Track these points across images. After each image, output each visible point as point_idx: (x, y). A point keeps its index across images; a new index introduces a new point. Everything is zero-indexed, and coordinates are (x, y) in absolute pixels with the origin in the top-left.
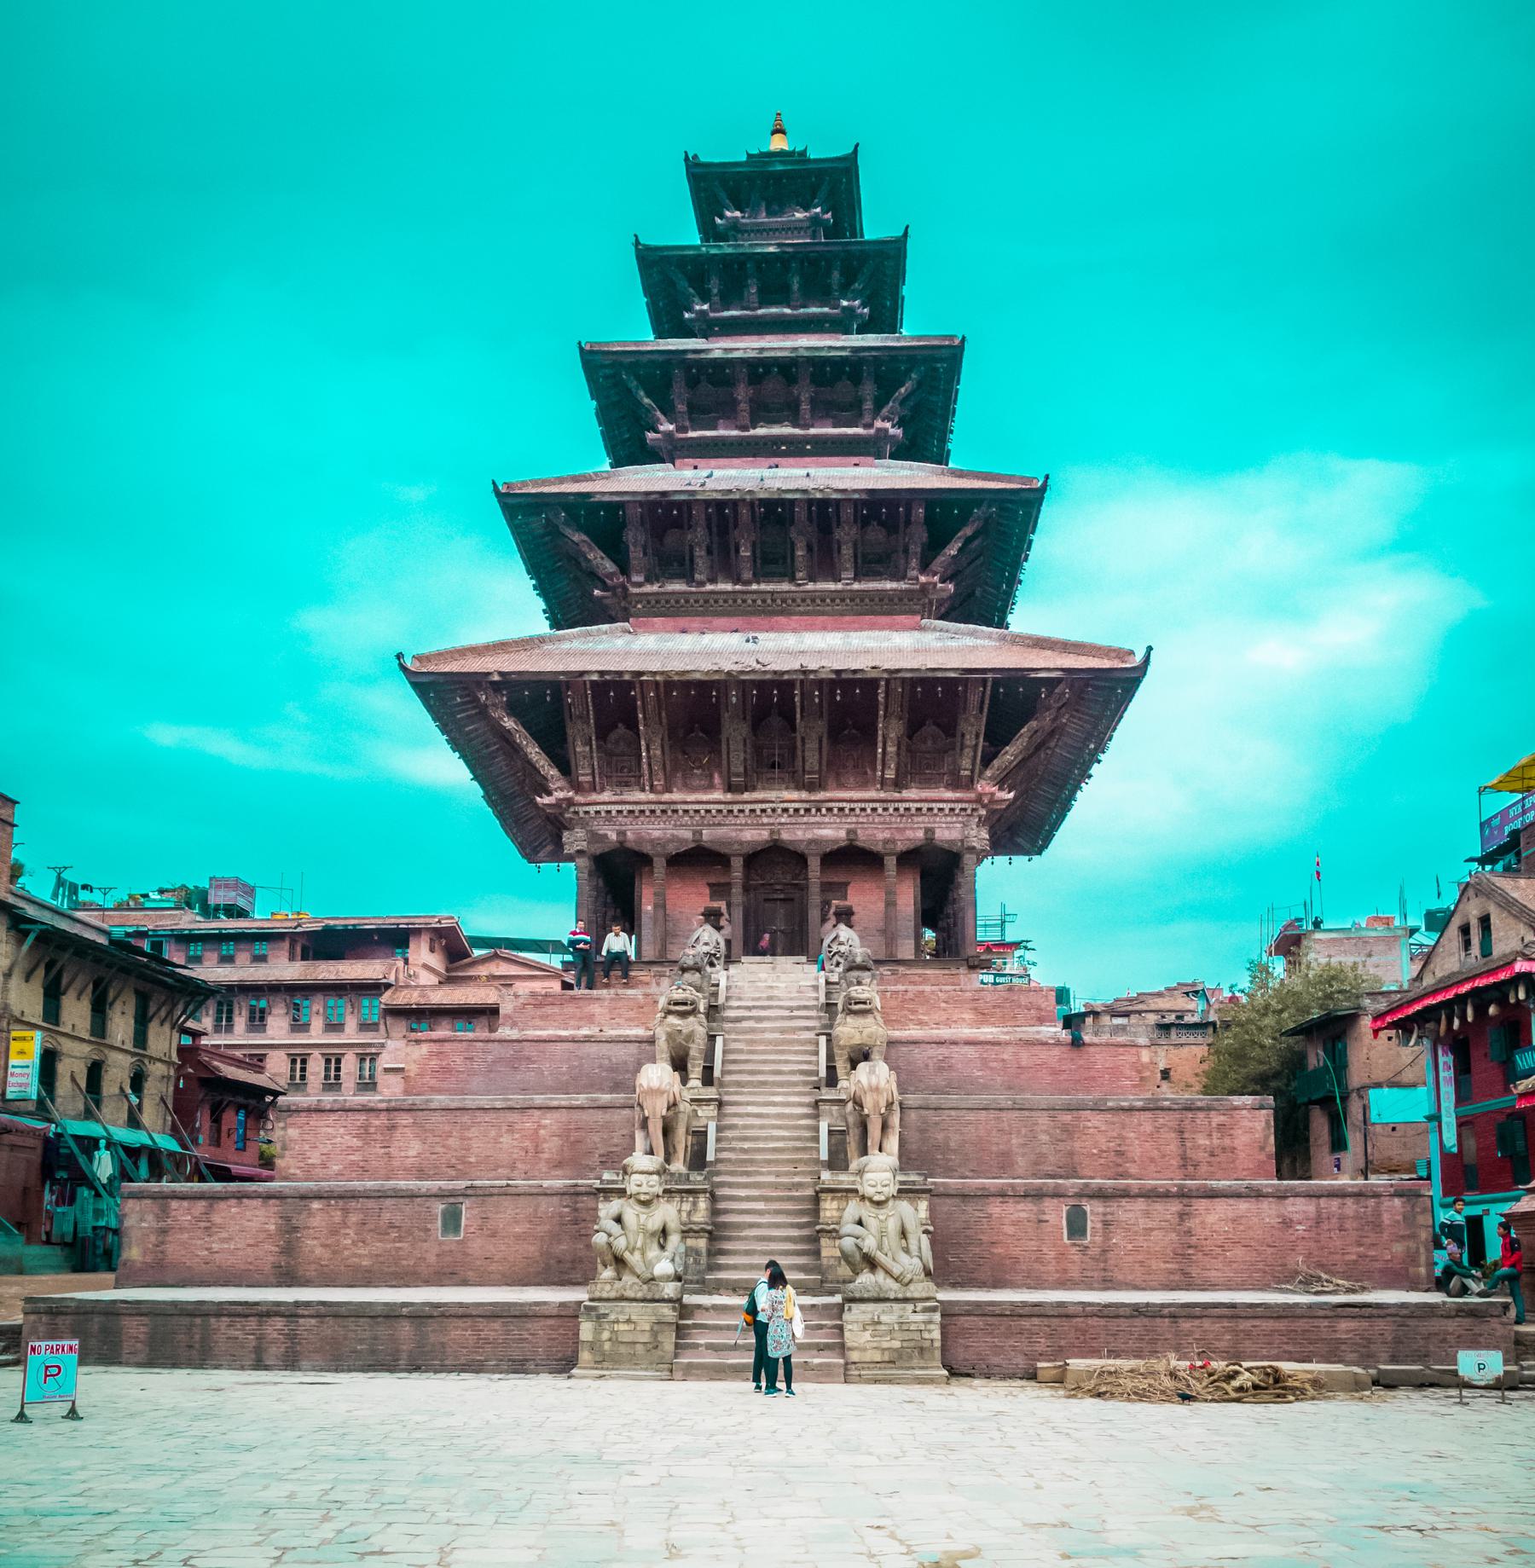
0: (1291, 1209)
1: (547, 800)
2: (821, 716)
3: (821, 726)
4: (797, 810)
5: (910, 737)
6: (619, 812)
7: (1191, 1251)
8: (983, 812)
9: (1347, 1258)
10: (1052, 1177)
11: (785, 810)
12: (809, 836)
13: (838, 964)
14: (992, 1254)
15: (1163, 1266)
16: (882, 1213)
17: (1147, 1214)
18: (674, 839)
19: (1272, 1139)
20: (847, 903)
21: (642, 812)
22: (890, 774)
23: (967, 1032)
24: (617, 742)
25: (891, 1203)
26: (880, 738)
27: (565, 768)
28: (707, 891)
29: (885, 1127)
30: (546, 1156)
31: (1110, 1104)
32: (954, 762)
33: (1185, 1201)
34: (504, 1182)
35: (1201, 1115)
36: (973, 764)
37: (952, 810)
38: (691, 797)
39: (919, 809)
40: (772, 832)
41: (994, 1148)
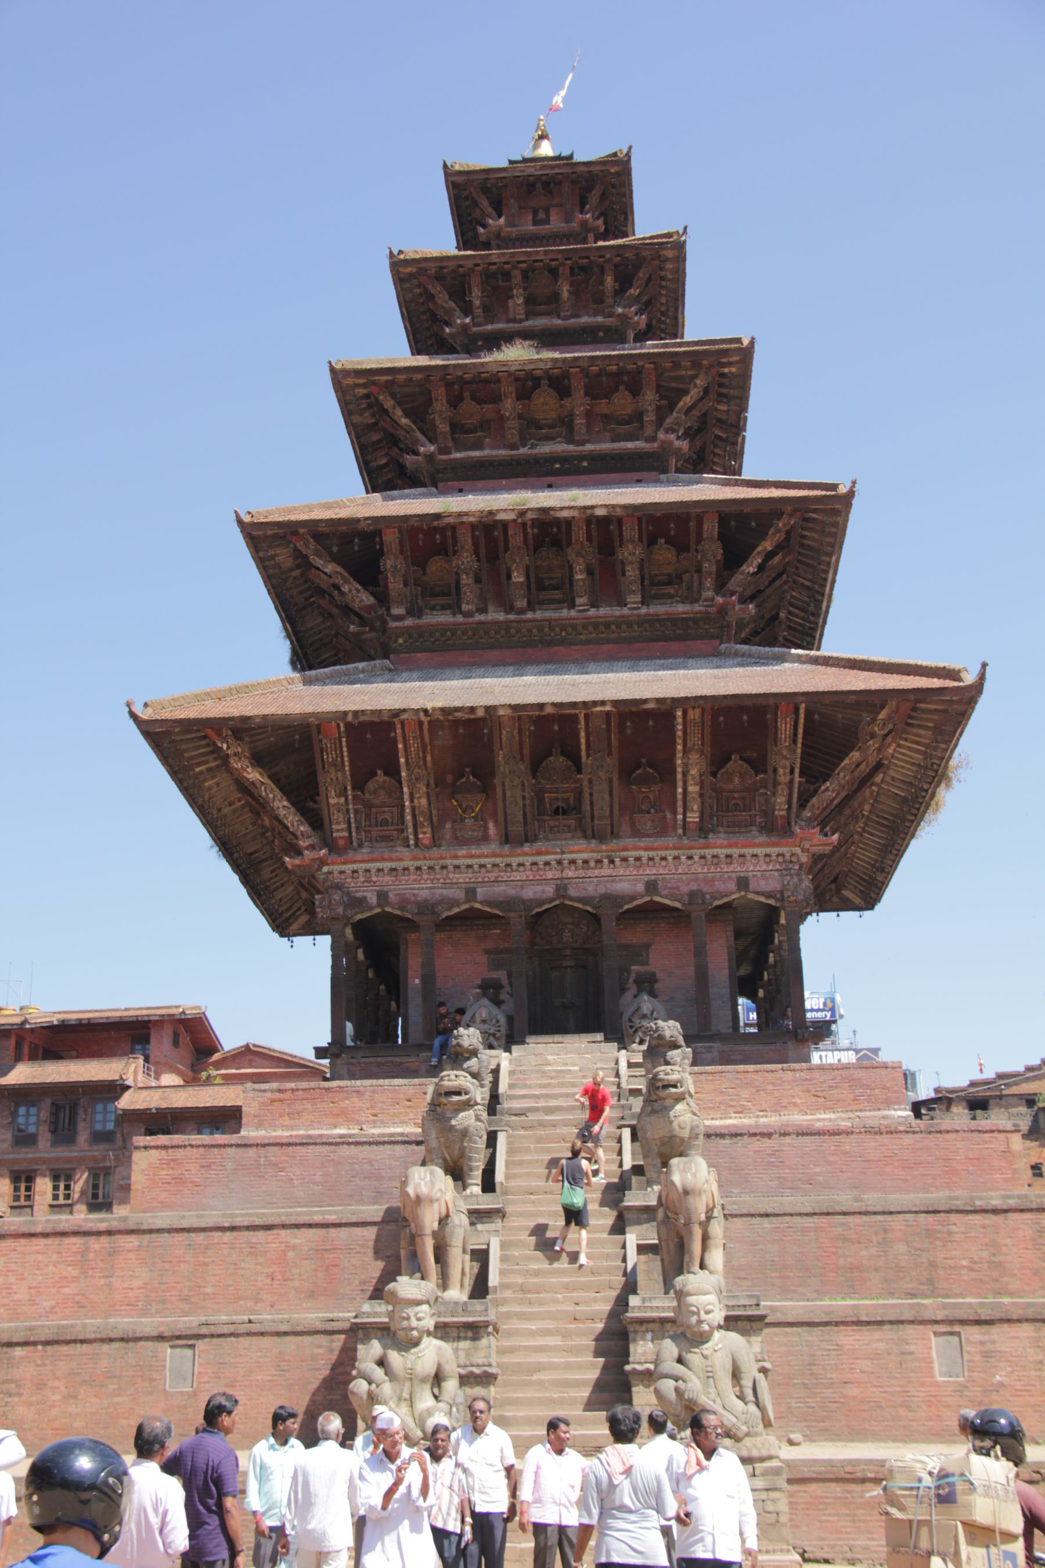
1: (297, 862)
2: (610, 753)
3: (611, 762)
4: (586, 862)
5: (714, 774)
6: (379, 870)
10: (913, 1296)
11: (573, 862)
12: (601, 890)
13: (641, 1042)
14: (845, 1397)
16: (707, 1348)
20: (649, 969)
21: (405, 869)
22: (693, 817)
23: (798, 1118)
25: (717, 1335)
26: (679, 777)
27: (316, 821)
28: (484, 959)
29: (705, 1238)
30: (296, 1284)
31: (978, 1203)
32: (767, 801)
34: (246, 1318)
37: (767, 855)
39: (729, 856)
40: (558, 888)
41: (841, 1262)
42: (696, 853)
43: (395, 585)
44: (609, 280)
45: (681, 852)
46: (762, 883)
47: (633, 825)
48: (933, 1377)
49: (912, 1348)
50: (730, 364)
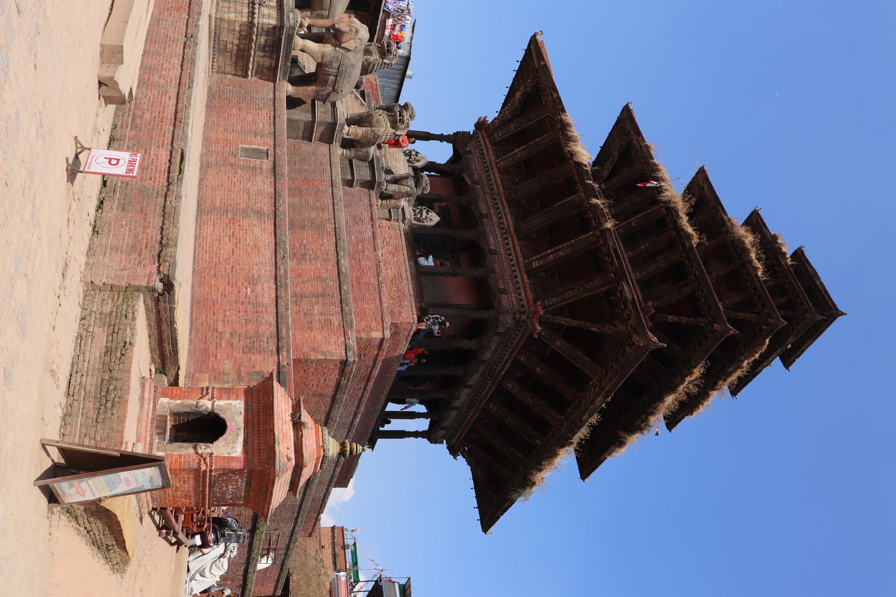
0: (265, 284)
4: (502, 223)
9: (220, 324)
11: (501, 218)
12: (488, 232)
15: (218, 198)
17: (260, 193)
19: (323, 357)
22: (535, 264)
31: (342, 253)
33: (272, 216)
35: (338, 309)
36: (554, 304)
37: (521, 300)
39: (517, 283)
41: (304, 187)
44: (783, 300)
46: (505, 301)
49: (259, 138)
50: (768, 325)
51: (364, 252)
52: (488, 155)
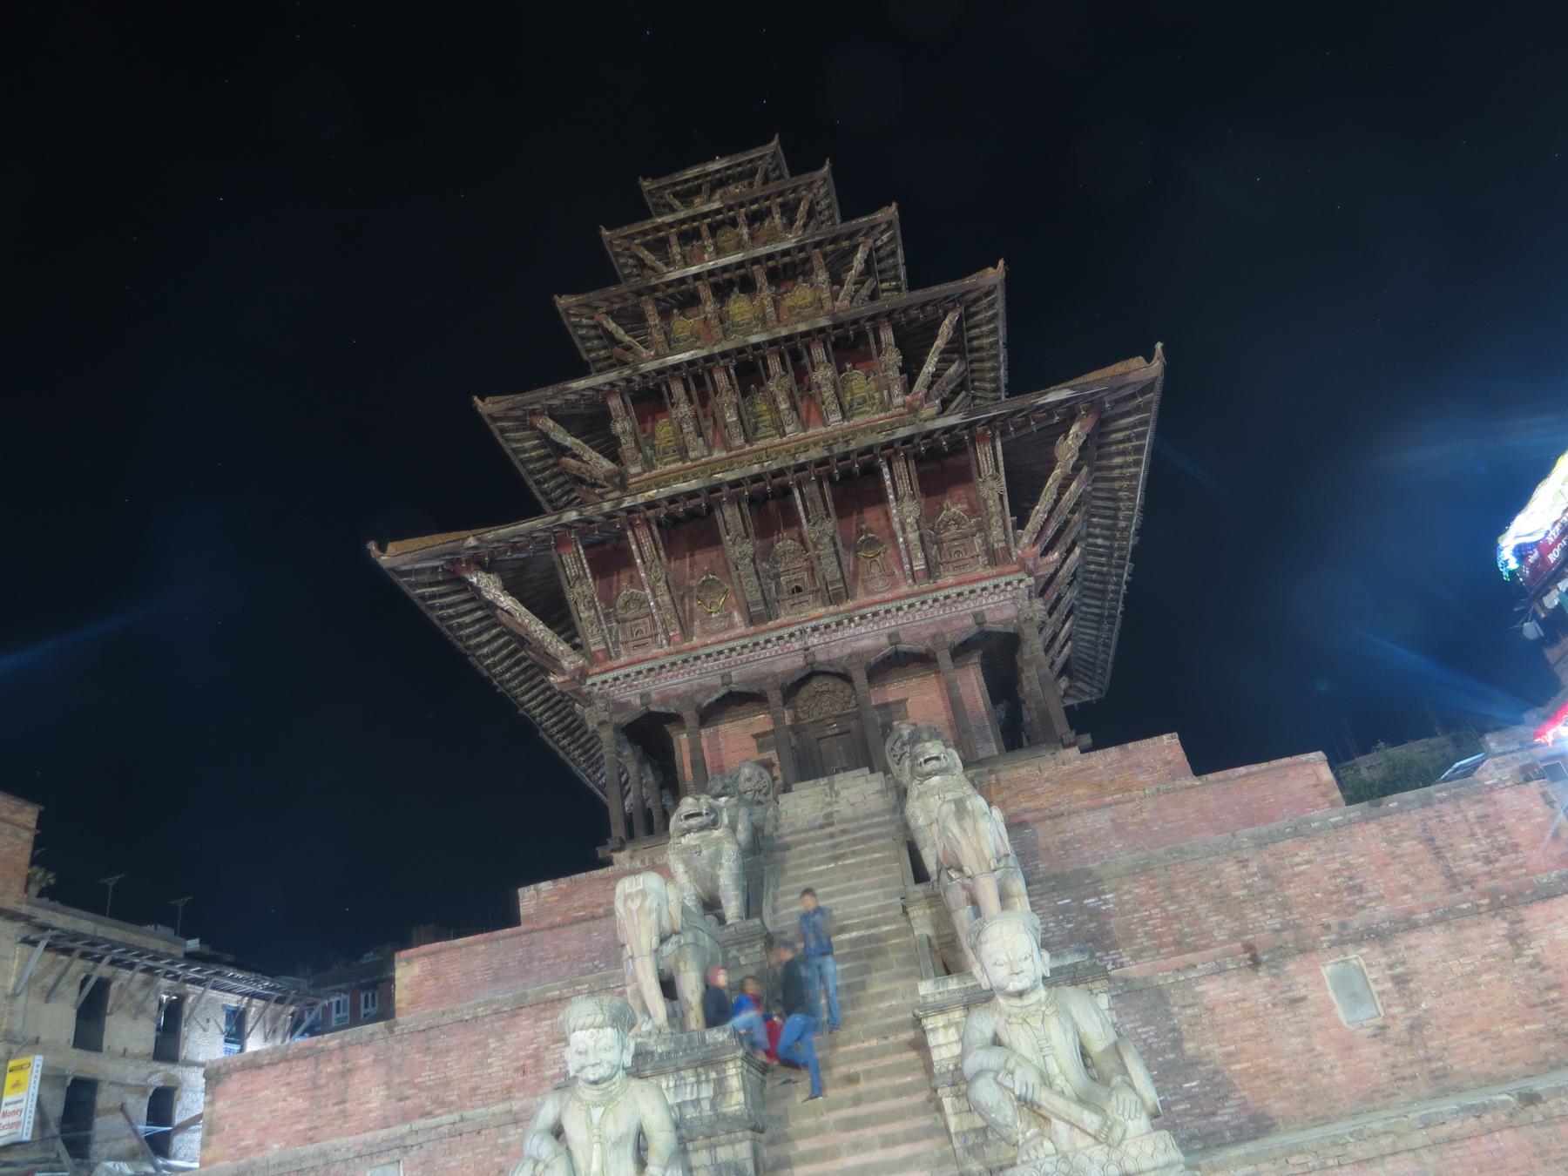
1: (560, 679)
2: (828, 515)
4: (827, 626)
7: (1554, 995)
8: (1031, 581)
11: (815, 629)
12: (848, 651)
15: (1519, 1030)
18: (702, 688)
21: (662, 667)
22: (919, 565)
24: (626, 606)
28: (753, 743)
37: (996, 586)
38: (713, 639)
39: (960, 595)
42: (929, 598)
43: (627, 444)
45: (913, 600)
47: (866, 589)
48: (1339, 1025)
49: (1303, 992)
51: (1144, 822)
52: (655, 658)
